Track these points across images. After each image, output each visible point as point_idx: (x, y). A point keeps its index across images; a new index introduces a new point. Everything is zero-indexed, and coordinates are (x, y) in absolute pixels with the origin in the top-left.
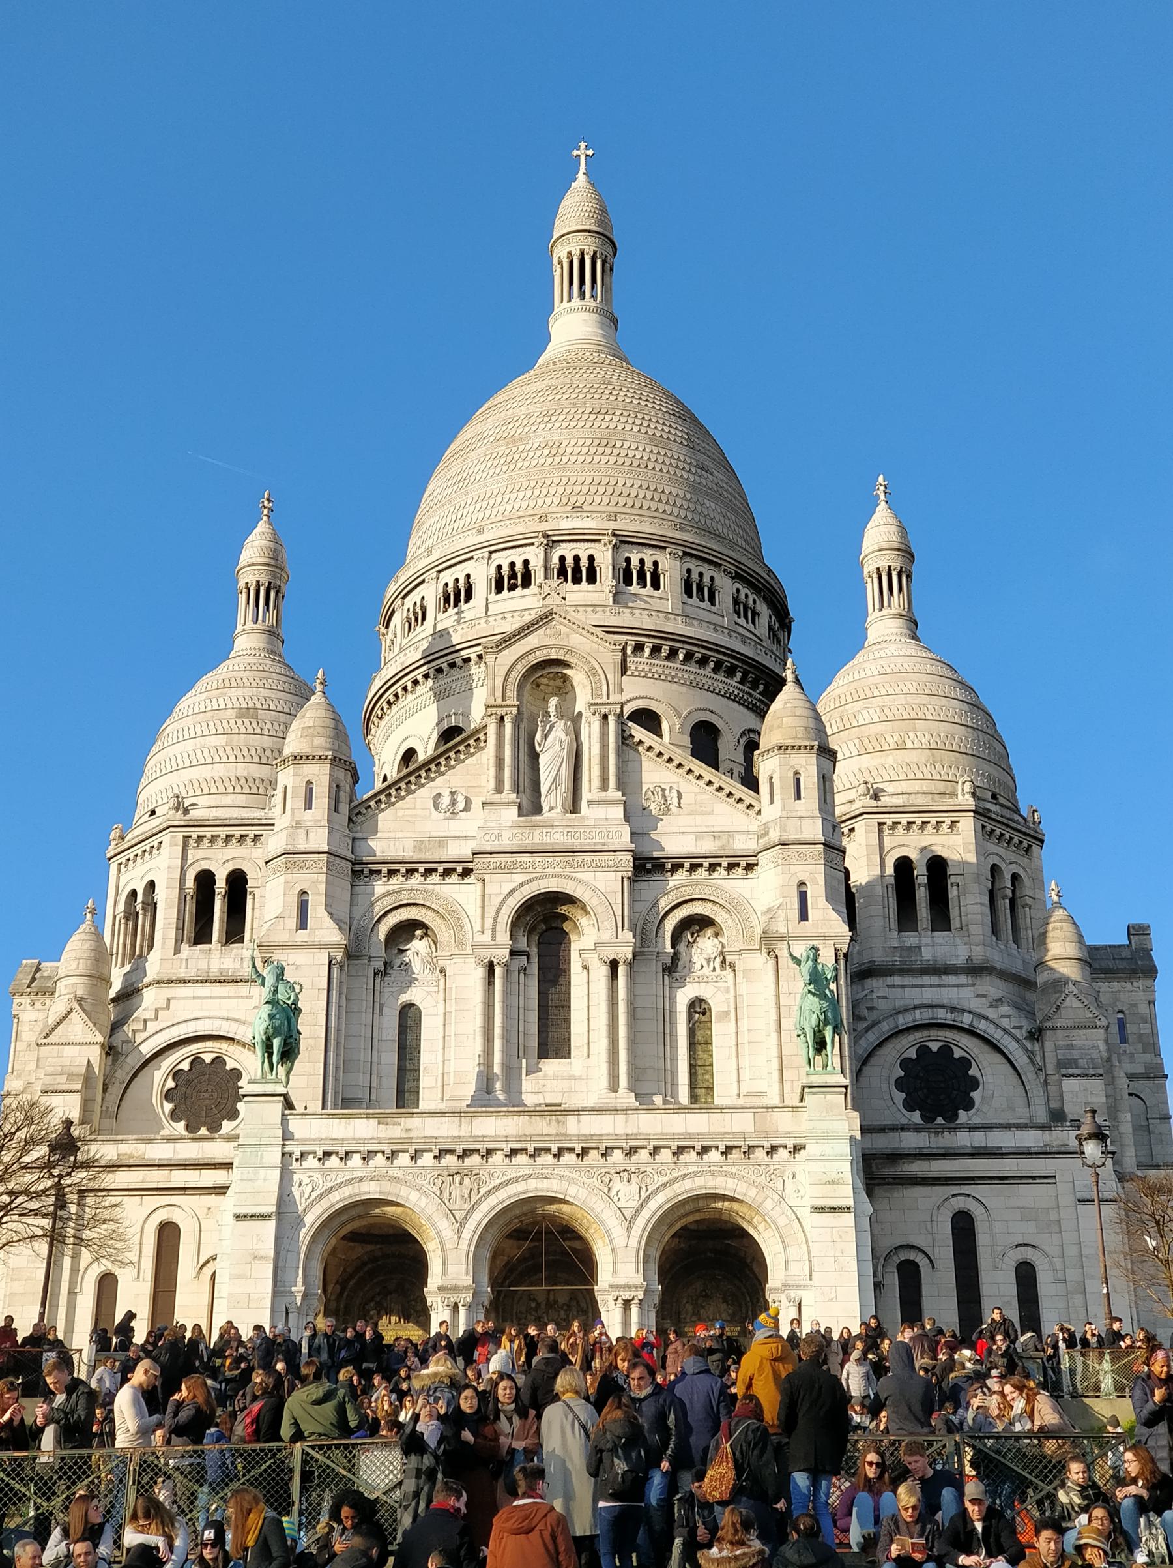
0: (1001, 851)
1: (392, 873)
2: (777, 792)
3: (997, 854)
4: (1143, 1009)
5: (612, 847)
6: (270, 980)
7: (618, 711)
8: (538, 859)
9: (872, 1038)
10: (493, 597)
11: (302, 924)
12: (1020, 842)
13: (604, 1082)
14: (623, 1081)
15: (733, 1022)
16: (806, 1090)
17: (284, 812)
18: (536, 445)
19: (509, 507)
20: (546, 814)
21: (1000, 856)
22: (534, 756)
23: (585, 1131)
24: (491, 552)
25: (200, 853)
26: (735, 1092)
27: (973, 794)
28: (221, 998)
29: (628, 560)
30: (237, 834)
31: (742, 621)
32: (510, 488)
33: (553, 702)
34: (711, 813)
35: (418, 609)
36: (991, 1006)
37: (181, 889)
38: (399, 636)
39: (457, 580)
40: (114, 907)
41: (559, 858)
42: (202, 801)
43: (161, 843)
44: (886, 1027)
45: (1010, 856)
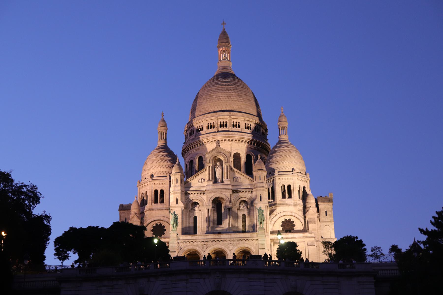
6: (173, 215)
9: (277, 218)
10: (207, 130)
11: (177, 203)
12: (305, 181)
15: (249, 218)
17: (173, 184)
23: (224, 237)
25: (155, 186)
29: (233, 122)
31: (256, 132)
37: (152, 193)
39: (200, 126)
41: (220, 191)
43: (147, 184)
44: (279, 216)
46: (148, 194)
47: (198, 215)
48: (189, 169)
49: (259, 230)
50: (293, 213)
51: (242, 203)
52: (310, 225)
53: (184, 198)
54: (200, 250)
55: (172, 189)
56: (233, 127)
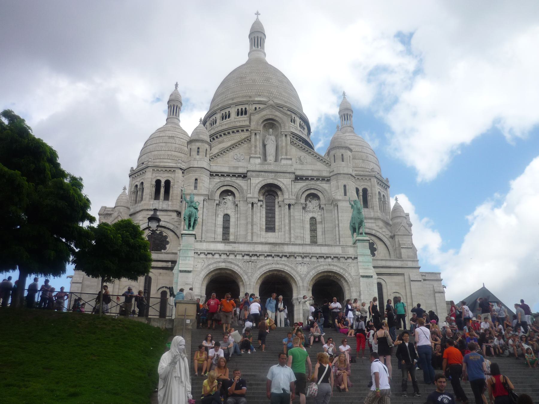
0: (380, 188)
5: (288, 171)
8: (266, 174)
11: (196, 187)
16: (357, 241)
19: (241, 95)
24: (236, 105)
25: (157, 175)
28: (162, 215)
30: (168, 170)
31: (301, 130)
32: (241, 90)
34: (316, 165)
36: (380, 229)
38: (208, 127)
39: (226, 113)
42: (158, 160)
45: (382, 190)
46: (145, 185)
47: (232, 213)
49: (359, 240)
50: (374, 231)
51: (309, 199)
52: (403, 251)
54: (241, 272)
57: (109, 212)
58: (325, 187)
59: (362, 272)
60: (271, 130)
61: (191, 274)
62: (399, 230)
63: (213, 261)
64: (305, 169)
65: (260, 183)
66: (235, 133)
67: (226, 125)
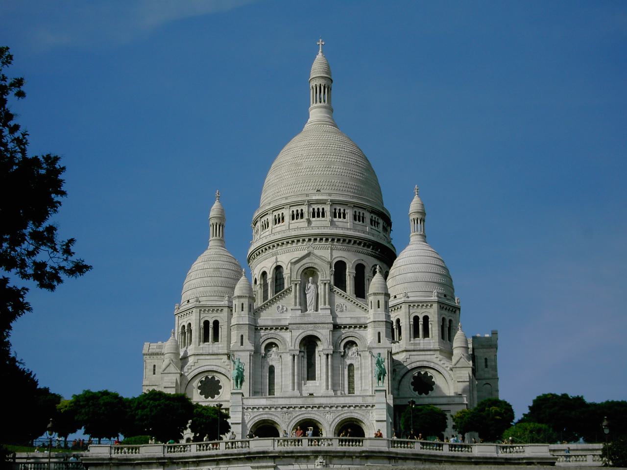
1: (266, 329)
2: (373, 306)
3: (445, 314)
4: (493, 357)
5: (327, 322)
6: (237, 363)
7: (329, 282)
11: (242, 344)
13: (324, 388)
14: (330, 387)
18: (304, 167)
20: (307, 312)
21: (445, 314)
22: (305, 294)
25: (205, 315)
26: (360, 389)
27: (438, 296)
29: (335, 209)
31: (373, 227)
33: (311, 278)
35: (266, 223)
37: (200, 326)
39: (279, 215)
40: (178, 330)
42: (204, 299)
46: (193, 327)
48: (259, 286)
51: (348, 346)
53: (254, 336)
55: (234, 321)
56: (335, 217)
57: (154, 351)
58: (361, 334)
59: (376, 417)
60: (311, 278)
61: (241, 425)
62: (458, 362)
63: (258, 414)
64: (343, 316)
65: (301, 335)
66: (291, 244)
67: (279, 234)
